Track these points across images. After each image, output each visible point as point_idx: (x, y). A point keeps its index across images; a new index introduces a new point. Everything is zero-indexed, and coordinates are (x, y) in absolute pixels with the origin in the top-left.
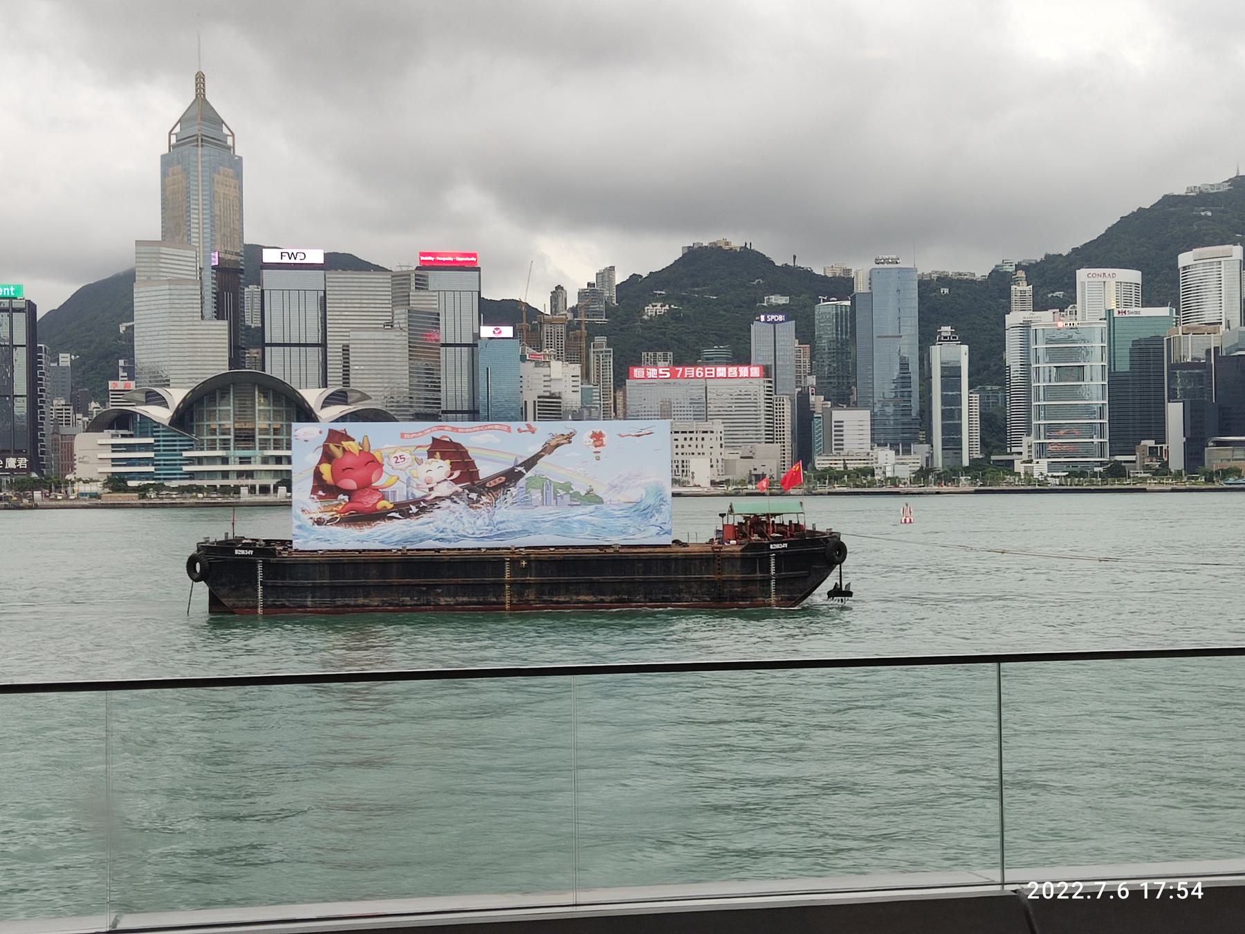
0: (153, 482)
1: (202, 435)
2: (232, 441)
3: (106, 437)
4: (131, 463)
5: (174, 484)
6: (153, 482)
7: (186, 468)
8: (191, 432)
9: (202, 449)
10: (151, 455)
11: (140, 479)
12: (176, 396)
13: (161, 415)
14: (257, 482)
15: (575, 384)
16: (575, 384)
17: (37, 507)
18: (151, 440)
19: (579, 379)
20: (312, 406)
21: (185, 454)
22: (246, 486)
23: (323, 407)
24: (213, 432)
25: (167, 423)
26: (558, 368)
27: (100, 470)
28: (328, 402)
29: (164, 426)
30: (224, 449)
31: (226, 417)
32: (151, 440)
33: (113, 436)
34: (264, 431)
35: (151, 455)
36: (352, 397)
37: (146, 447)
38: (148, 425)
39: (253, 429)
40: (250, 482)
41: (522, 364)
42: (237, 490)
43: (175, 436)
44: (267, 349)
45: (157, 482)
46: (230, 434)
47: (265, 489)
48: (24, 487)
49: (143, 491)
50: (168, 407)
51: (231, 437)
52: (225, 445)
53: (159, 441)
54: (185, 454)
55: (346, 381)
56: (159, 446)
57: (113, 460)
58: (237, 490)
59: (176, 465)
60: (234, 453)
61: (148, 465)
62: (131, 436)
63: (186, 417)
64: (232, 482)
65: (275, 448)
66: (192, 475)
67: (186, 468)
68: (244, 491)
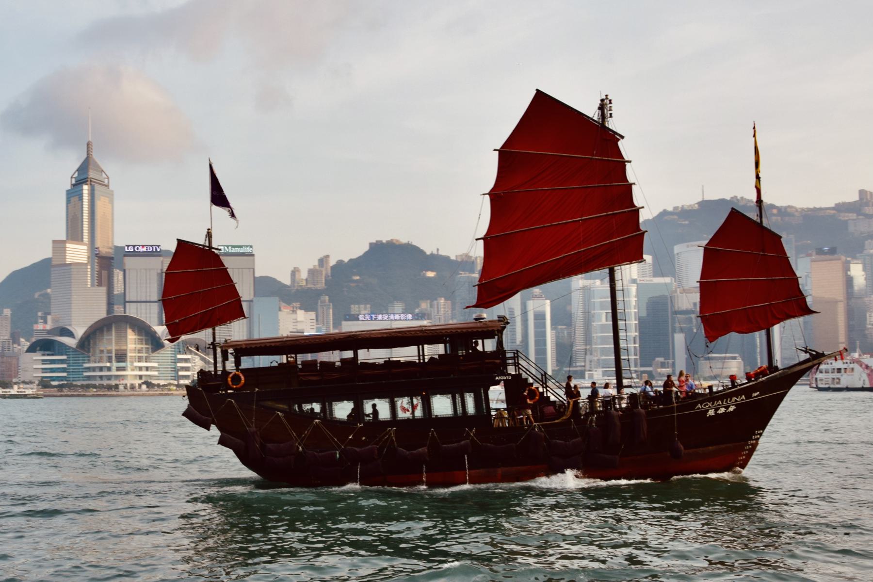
0: (65, 382)
3: (38, 356)
4: (52, 370)
5: (79, 383)
7: (86, 374)
11: (59, 381)
15: (312, 324)
16: (312, 324)
18: (64, 357)
19: (314, 321)
24: (102, 351)
26: (301, 315)
27: (35, 375)
29: (73, 348)
31: (109, 343)
32: (64, 357)
33: (44, 355)
34: (131, 351)
35: (65, 366)
38: (62, 349)
39: (126, 350)
41: (280, 312)
43: (79, 354)
44: (127, 304)
49: (60, 387)
52: (110, 360)
53: (70, 357)
56: (70, 360)
57: (43, 369)
58: (116, 387)
59: (79, 372)
60: (115, 365)
62: (53, 355)
64: (113, 382)
67: (86, 374)
68: (121, 387)
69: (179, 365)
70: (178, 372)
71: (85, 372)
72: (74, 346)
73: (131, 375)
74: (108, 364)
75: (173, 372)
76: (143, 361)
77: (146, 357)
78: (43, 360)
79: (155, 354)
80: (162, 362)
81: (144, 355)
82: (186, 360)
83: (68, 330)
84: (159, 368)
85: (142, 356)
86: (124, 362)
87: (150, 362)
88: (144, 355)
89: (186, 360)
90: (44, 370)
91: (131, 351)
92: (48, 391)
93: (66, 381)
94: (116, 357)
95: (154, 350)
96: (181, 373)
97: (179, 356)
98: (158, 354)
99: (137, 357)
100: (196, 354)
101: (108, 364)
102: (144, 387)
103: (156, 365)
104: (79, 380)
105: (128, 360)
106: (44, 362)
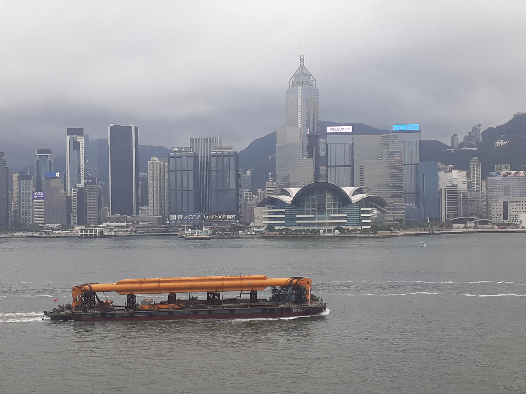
0: (284, 227)
1: (304, 208)
2: (316, 210)
3: (266, 209)
4: (275, 219)
5: (293, 228)
6: (284, 227)
7: (297, 222)
8: (299, 207)
9: (304, 214)
10: (284, 216)
12: (294, 191)
13: (288, 199)
14: (327, 228)
17: (240, 238)
18: (284, 210)
20: (349, 195)
21: (297, 216)
22: (322, 229)
23: (353, 195)
25: (290, 203)
28: (355, 193)
29: (289, 204)
30: (313, 214)
32: (284, 210)
33: (269, 208)
34: (329, 206)
35: (284, 216)
36: (365, 190)
37: (282, 213)
38: (282, 204)
40: (324, 228)
42: (319, 230)
45: (286, 228)
46: (315, 208)
47: (330, 231)
48: (236, 229)
50: (290, 196)
51: (316, 209)
52: (313, 212)
54: (297, 216)
55: (362, 184)
57: (269, 218)
58: (319, 230)
59: (294, 220)
61: (282, 220)
62: (276, 208)
63: (297, 200)
64: (316, 228)
65: (334, 214)
66: (300, 225)
67: (297, 222)
68: (321, 231)
69: (362, 215)
70: (361, 221)
71: (298, 220)
72: (290, 203)
73: (328, 223)
74: (312, 216)
75: (358, 220)
76: (337, 214)
77: (339, 210)
78: (269, 212)
79: (344, 208)
80: (350, 213)
81: (337, 209)
82: (368, 212)
83: (286, 191)
84: (348, 218)
85: (337, 210)
86: (323, 214)
87: (341, 214)
88: (337, 209)
89: (368, 212)
90: (270, 219)
91: (329, 206)
92: (272, 234)
93: (285, 226)
94: (318, 210)
95: (344, 206)
96: (363, 221)
97: (362, 209)
98: (348, 208)
99: (332, 210)
100: (376, 207)
101: (312, 216)
102: (337, 231)
103: (346, 215)
104: (293, 226)
105: (326, 212)
106: (270, 213)
